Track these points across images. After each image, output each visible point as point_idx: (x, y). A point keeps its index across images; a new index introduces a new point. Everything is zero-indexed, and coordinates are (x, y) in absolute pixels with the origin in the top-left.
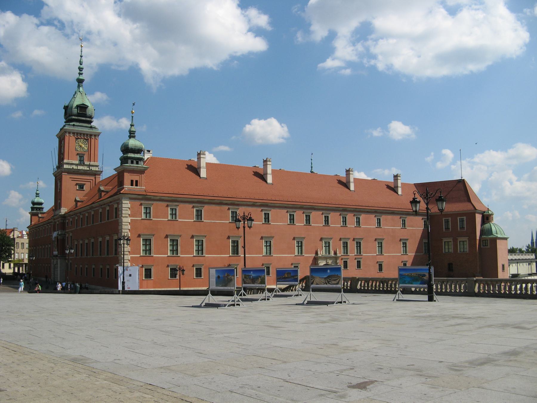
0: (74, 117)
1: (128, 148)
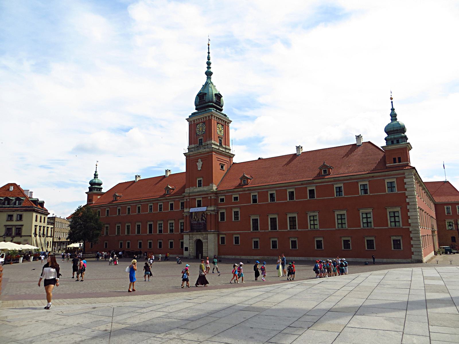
0: (214, 104)
1: (404, 128)
